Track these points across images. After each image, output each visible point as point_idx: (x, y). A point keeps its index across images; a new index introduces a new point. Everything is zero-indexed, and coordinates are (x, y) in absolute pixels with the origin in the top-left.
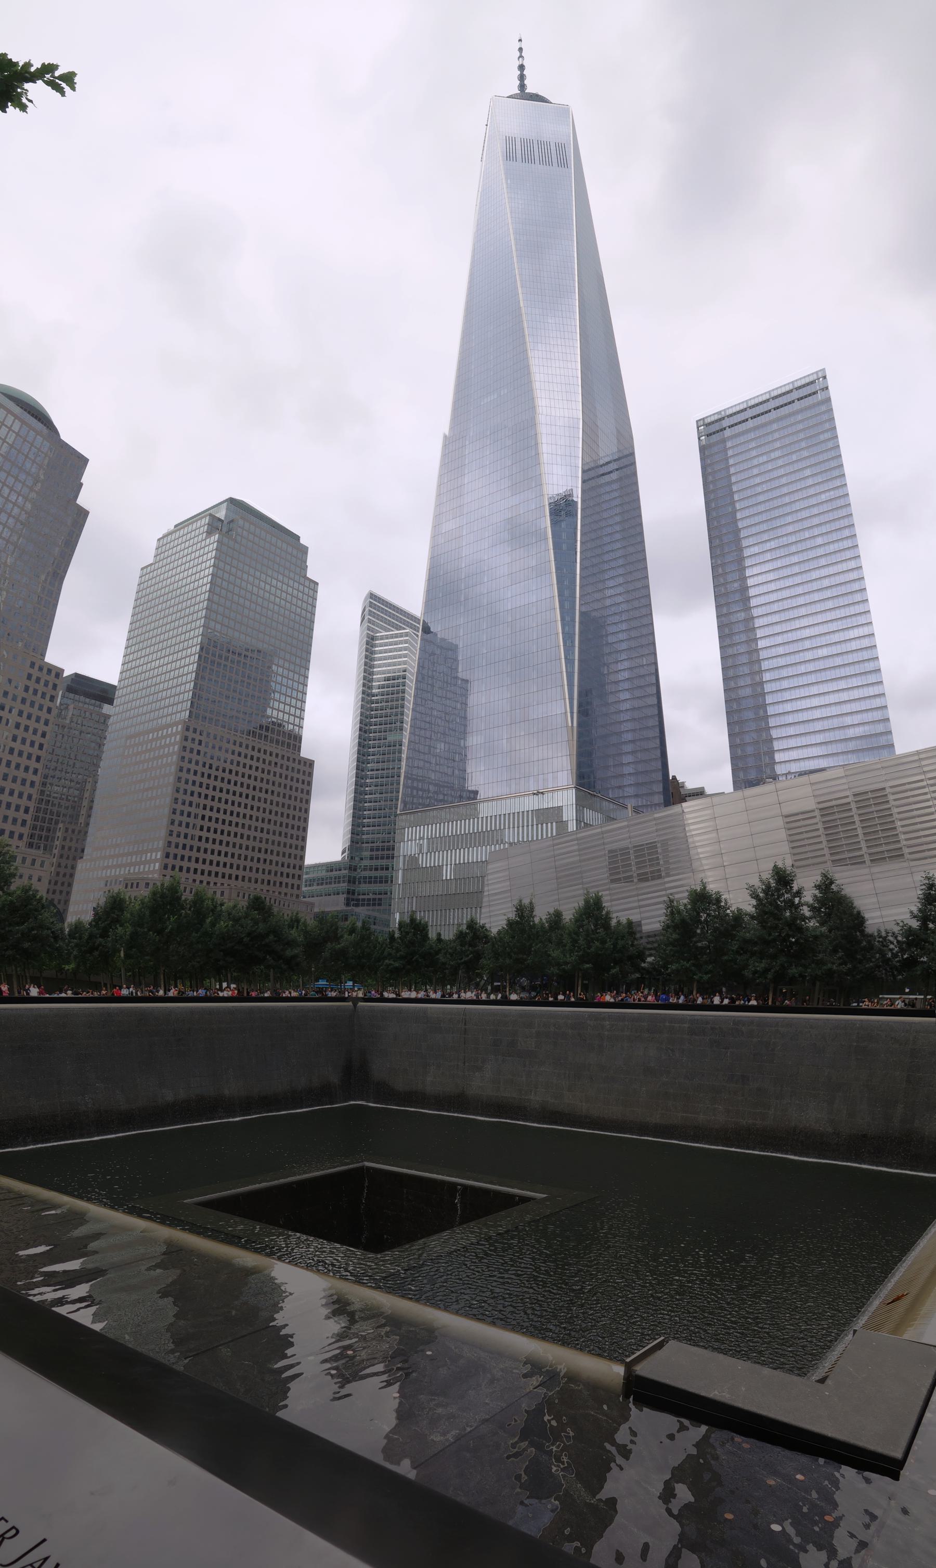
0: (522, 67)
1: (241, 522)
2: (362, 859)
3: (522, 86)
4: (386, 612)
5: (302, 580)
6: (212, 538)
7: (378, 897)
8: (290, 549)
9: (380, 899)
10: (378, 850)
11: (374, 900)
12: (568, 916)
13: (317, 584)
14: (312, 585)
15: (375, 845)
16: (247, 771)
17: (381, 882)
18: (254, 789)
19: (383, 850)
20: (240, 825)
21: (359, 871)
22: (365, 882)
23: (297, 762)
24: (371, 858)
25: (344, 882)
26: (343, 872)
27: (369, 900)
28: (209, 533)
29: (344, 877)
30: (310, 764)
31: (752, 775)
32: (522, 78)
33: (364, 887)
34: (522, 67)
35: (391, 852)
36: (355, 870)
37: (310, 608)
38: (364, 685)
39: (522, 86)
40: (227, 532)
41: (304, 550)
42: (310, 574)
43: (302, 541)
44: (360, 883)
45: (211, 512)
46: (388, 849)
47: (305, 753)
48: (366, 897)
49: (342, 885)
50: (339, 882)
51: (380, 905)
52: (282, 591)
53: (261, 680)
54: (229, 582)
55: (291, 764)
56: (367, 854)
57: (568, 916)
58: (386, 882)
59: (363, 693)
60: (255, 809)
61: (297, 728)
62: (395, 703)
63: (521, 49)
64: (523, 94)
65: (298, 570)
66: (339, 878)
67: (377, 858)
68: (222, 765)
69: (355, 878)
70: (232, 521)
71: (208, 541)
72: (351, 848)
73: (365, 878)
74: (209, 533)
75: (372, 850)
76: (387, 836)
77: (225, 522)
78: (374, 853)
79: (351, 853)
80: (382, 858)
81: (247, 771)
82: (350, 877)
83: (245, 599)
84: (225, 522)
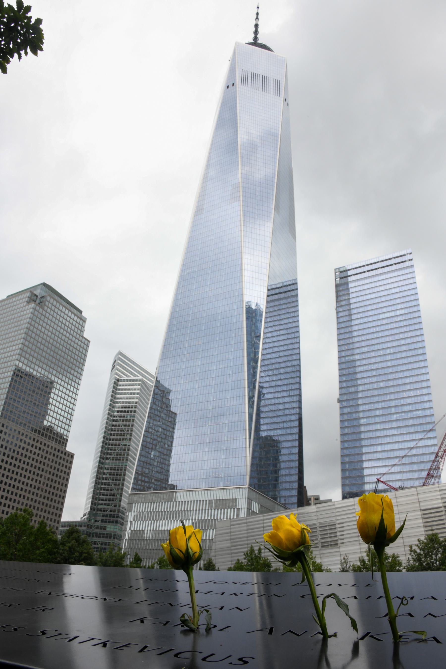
0: (256, 26)
1: (48, 298)
2: (96, 521)
3: (256, 38)
5: (81, 338)
6: (30, 306)
7: (104, 546)
8: (76, 318)
9: (105, 549)
10: (107, 516)
11: (101, 549)
13: (89, 341)
14: (86, 342)
15: (105, 513)
16: (32, 456)
17: (107, 537)
18: (35, 467)
19: (110, 517)
20: (24, 490)
21: (93, 528)
22: (96, 537)
23: (64, 453)
24: (102, 521)
27: (98, 548)
28: (28, 302)
29: (83, 531)
32: (256, 32)
34: (256, 26)
35: (115, 519)
36: (91, 528)
37: (83, 356)
38: (109, 409)
39: (256, 38)
40: (39, 303)
43: (83, 314)
44: (93, 536)
45: (31, 290)
46: (114, 517)
48: (96, 546)
52: (67, 343)
53: (44, 396)
54: (36, 334)
55: (60, 454)
56: (99, 518)
58: (110, 538)
59: (109, 414)
60: (34, 480)
61: (65, 432)
62: (128, 423)
63: (257, 14)
64: (255, 43)
65: (79, 332)
67: (106, 522)
68: (13, 448)
69: (90, 533)
70: (43, 297)
71: (27, 307)
72: (90, 513)
73: (96, 533)
74: (28, 302)
75: (103, 516)
76: (114, 508)
77: (39, 297)
78: (104, 518)
79: (89, 516)
80: (109, 522)
81: (32, 456)
83: (44, 346)
84: (39, 297)
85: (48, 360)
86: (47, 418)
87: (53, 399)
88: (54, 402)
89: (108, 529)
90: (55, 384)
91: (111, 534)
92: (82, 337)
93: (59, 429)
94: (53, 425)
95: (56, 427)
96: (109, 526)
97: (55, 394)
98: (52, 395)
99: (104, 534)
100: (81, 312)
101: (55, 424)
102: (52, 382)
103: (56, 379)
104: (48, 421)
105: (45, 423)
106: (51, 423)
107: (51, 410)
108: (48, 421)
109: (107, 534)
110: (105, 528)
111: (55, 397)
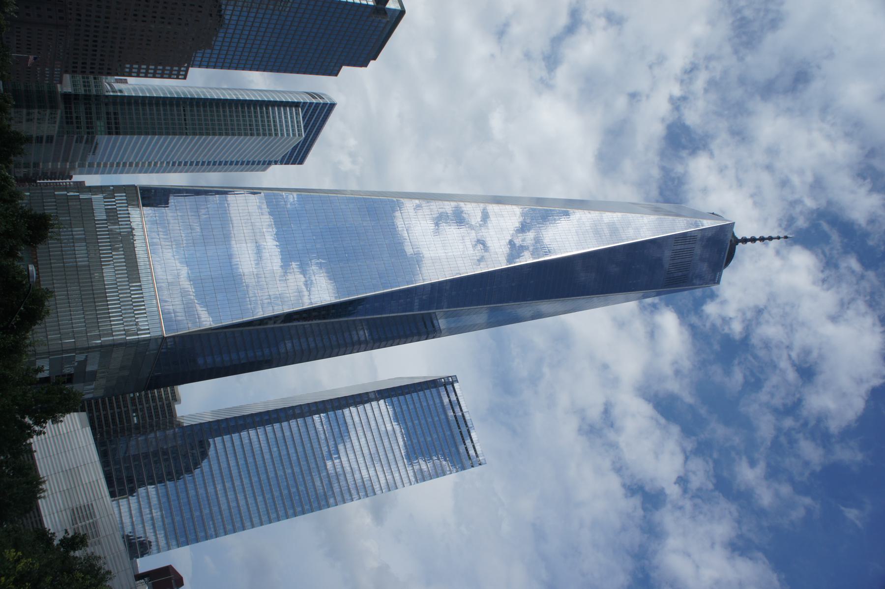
7: (74, 120)
9: (72, 123)
11: (71, 118)
25: (85, 91)
26: (94, 89)
27: (71, 113)
29: (90, 90)
33: (82, 108)
35: (114, 130)
44: (85, 104)
49: (83, 89)
50: (85, 86)
51: (67, 123)
58: (88, 128)
66: (89, 86)
73: (90, 109)
78: (112, 116)
80: (108, 123)
82: (90, 96)
89: (98, 123)
96: (102, 124)
99: (91, 118)
109: (91, 123)
110: (98, 118)
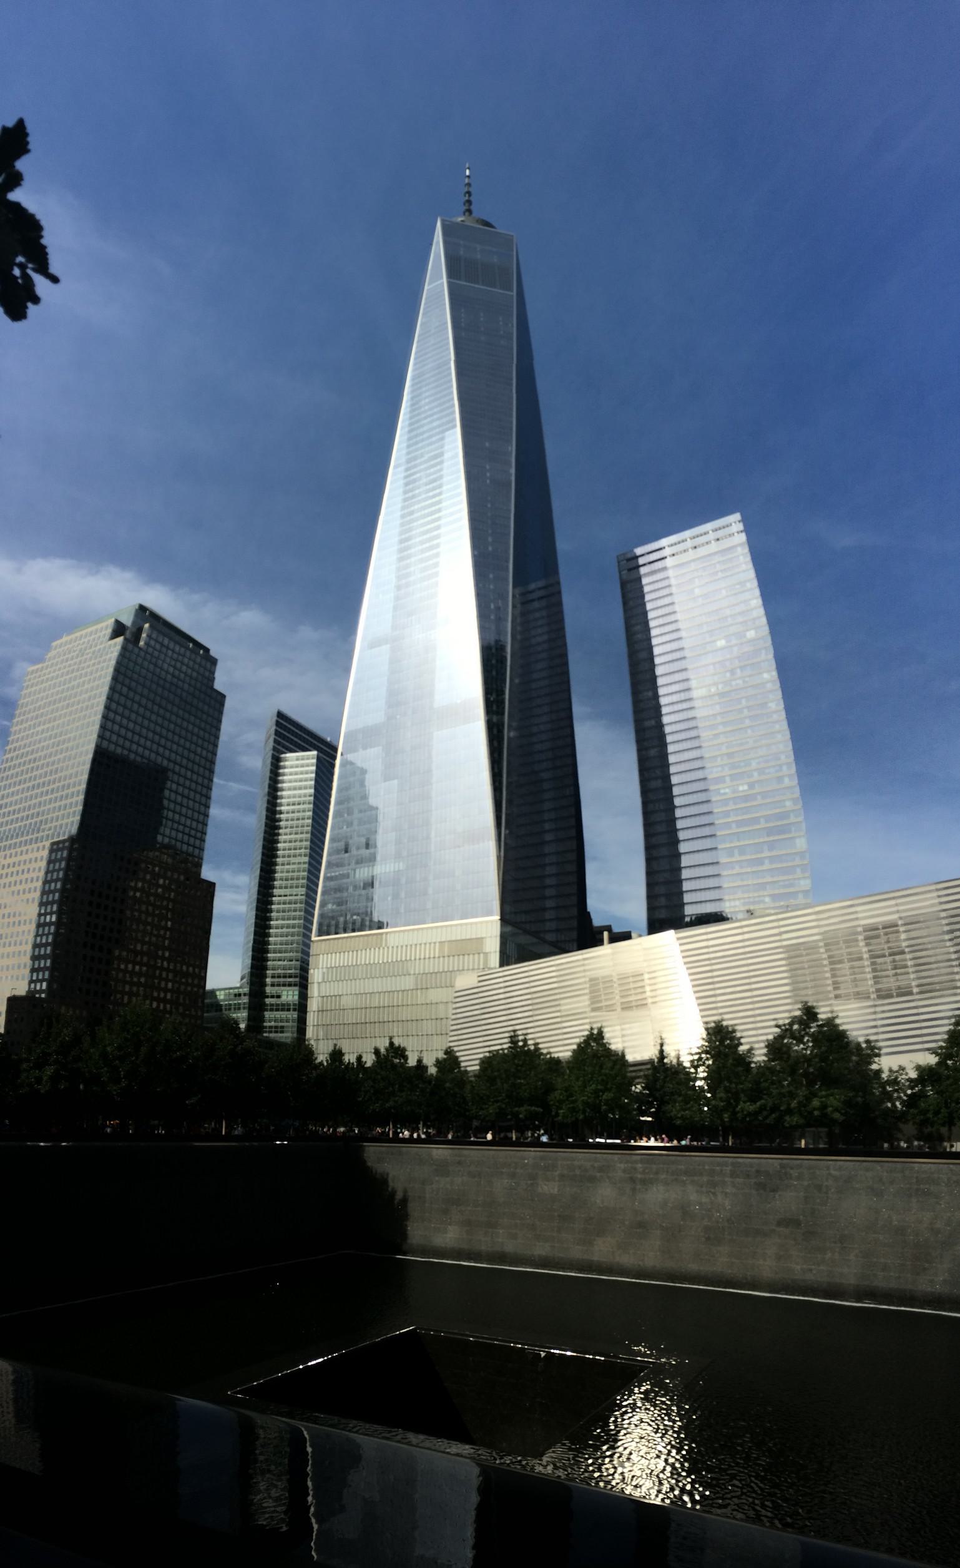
4: (293, 733)
9: (282, 1027)
10: (279, 977)
11: (276, 1027)
12: (470, 1063)
13: (224, 696)
30: (211, 886)
31: (662, 914)
41: (214, 662)
42: (218, 685)
43: (212, 653)
47: (208, 873)
57: (470, 1063)
67: (279, 985)
78: (276, 980)
80: (284, 985)
85: (154, 732)
86: (162, 831)
87: (169, 800)
88: (172, 806)
90: (170, 774)
91: (289, 1005)
92: (212, 688)
93: (185, 847)
94: (173, 842)
95: (179, 844)
97: (171, 790)
98: (167, 793)
99: (278, 1005)
100: (207, 650)
101: (176, 840)
102: (164, 771)
103: (171, 765)
104: (164, 835)
105: (159, 838)
106: (170, 837)
107: (167, 819)
108: (164, 835)
109: (283, 1005)
110: (279, 997)
111: (173, 796)
